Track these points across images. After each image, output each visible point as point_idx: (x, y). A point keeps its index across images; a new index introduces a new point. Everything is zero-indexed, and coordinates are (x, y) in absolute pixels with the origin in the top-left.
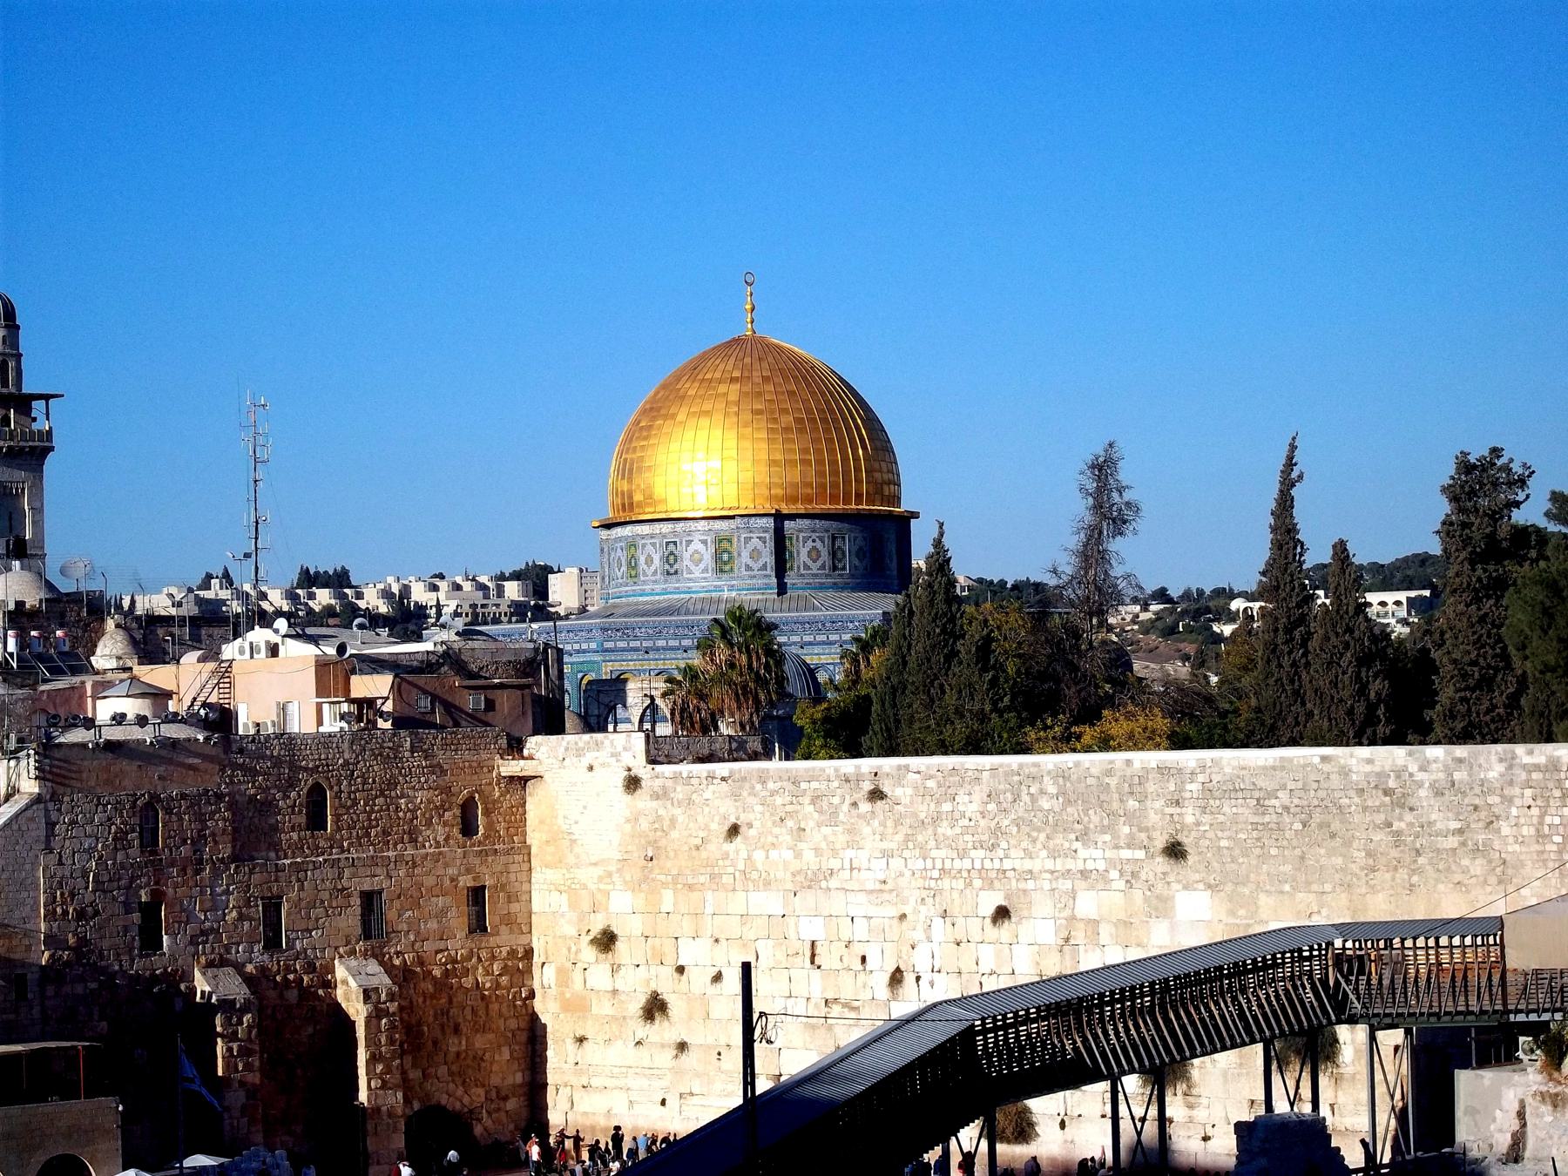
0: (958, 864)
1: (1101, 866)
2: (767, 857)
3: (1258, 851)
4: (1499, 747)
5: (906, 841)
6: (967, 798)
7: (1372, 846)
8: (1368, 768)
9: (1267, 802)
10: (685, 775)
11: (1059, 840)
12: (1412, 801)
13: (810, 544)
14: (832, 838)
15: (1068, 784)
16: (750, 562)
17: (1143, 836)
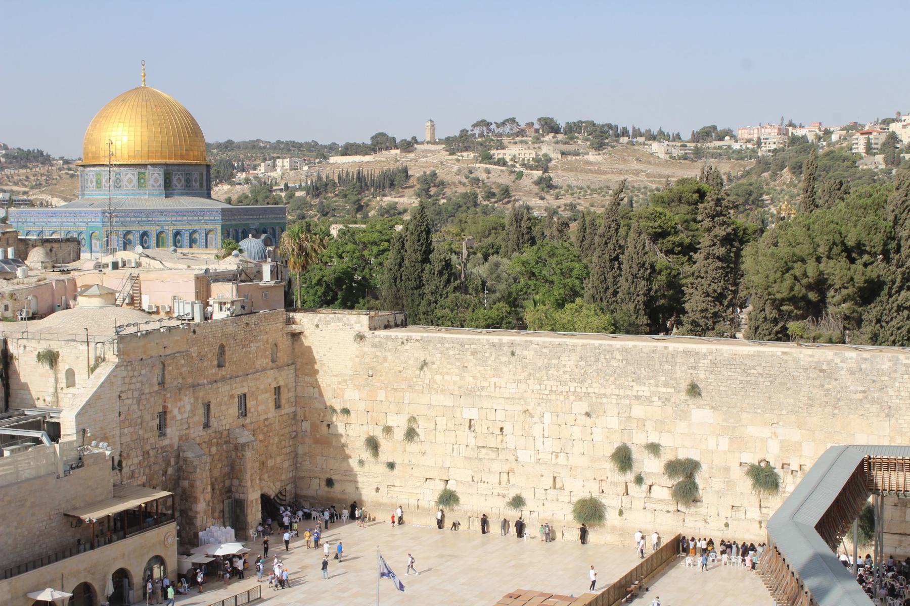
0: (560, 388)
1: (647, 394)
2: (443, 379)
3: (743, 393)
4: (890, 355)
5: (529, 376)
6: (567, 358)
7: (812, 395)
8: (811, 359)
9: (749, 371)
10: (393, 337)
11: (622, 381)
12: (836, 376)
13: (177, 176)
14: (484, 372)
15: (629, 356)
16: (154, 184)
17: (673, 382)
